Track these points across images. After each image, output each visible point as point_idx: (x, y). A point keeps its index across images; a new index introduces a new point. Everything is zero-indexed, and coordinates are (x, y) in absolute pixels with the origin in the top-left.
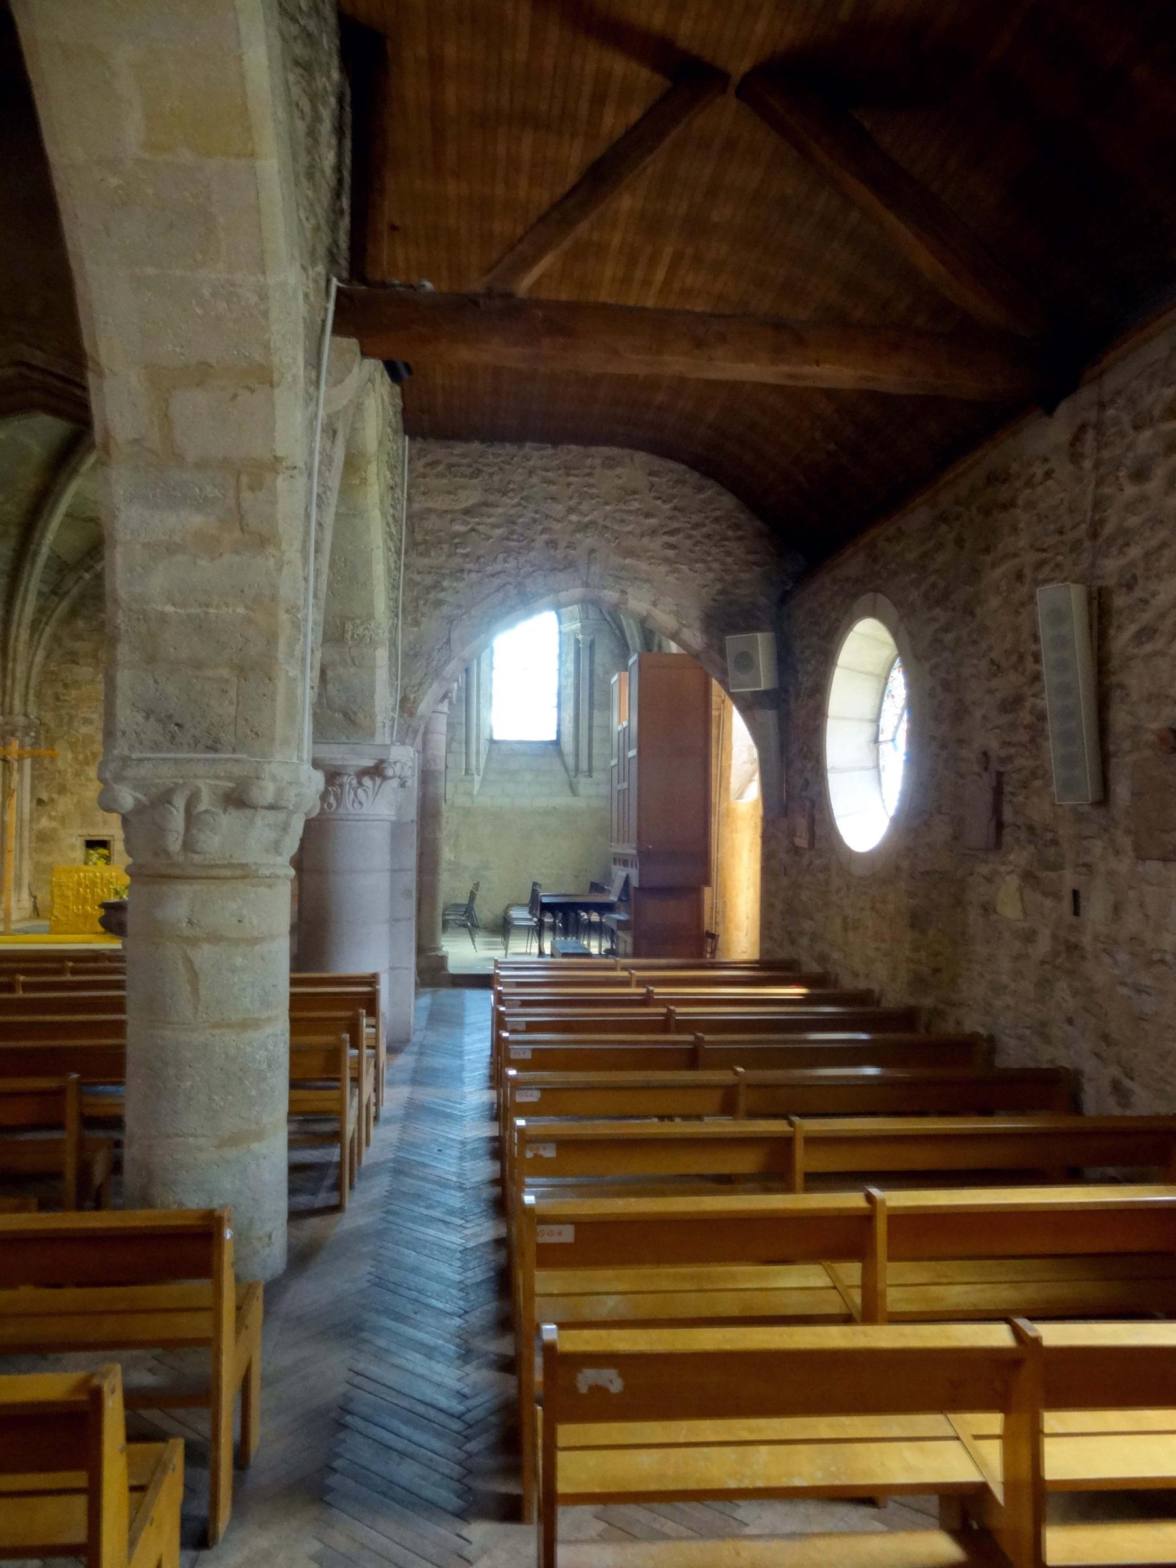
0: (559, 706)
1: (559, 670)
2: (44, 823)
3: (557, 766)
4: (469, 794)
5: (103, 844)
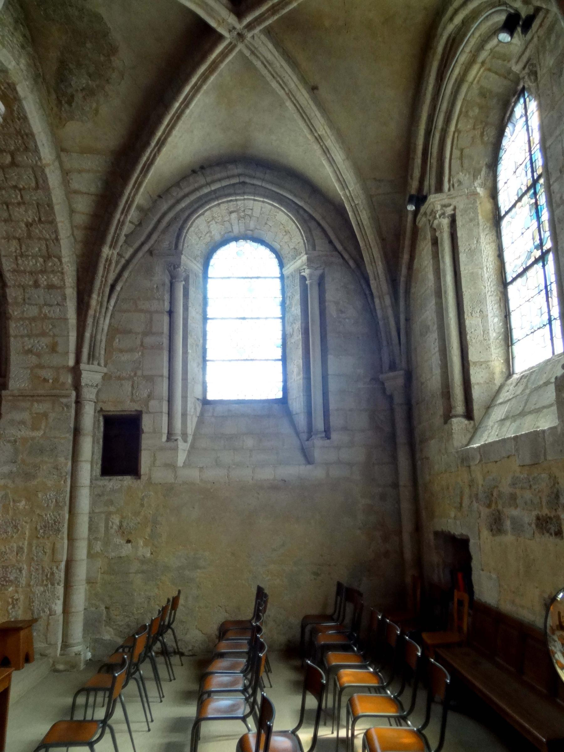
0: (284, 359)
1: (283, 318)
3: (285, 429)
4: (172, 466)
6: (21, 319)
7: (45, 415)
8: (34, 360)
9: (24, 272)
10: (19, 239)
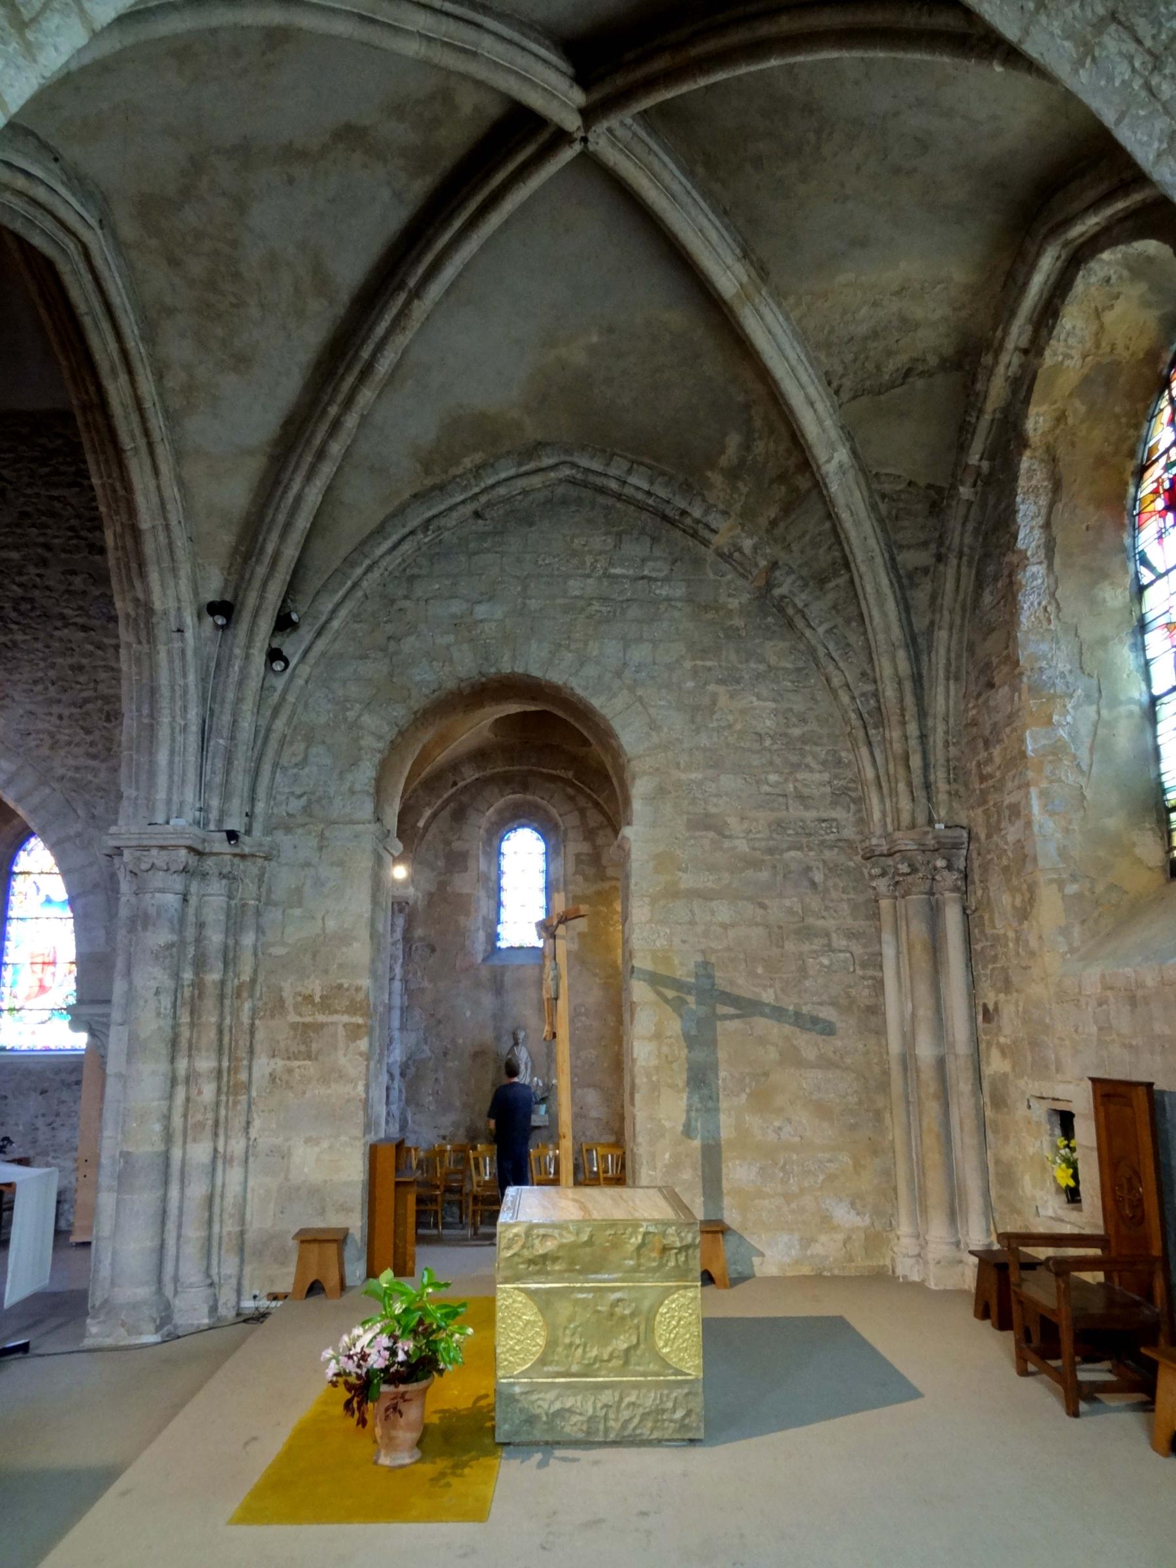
10: (1113, 17)
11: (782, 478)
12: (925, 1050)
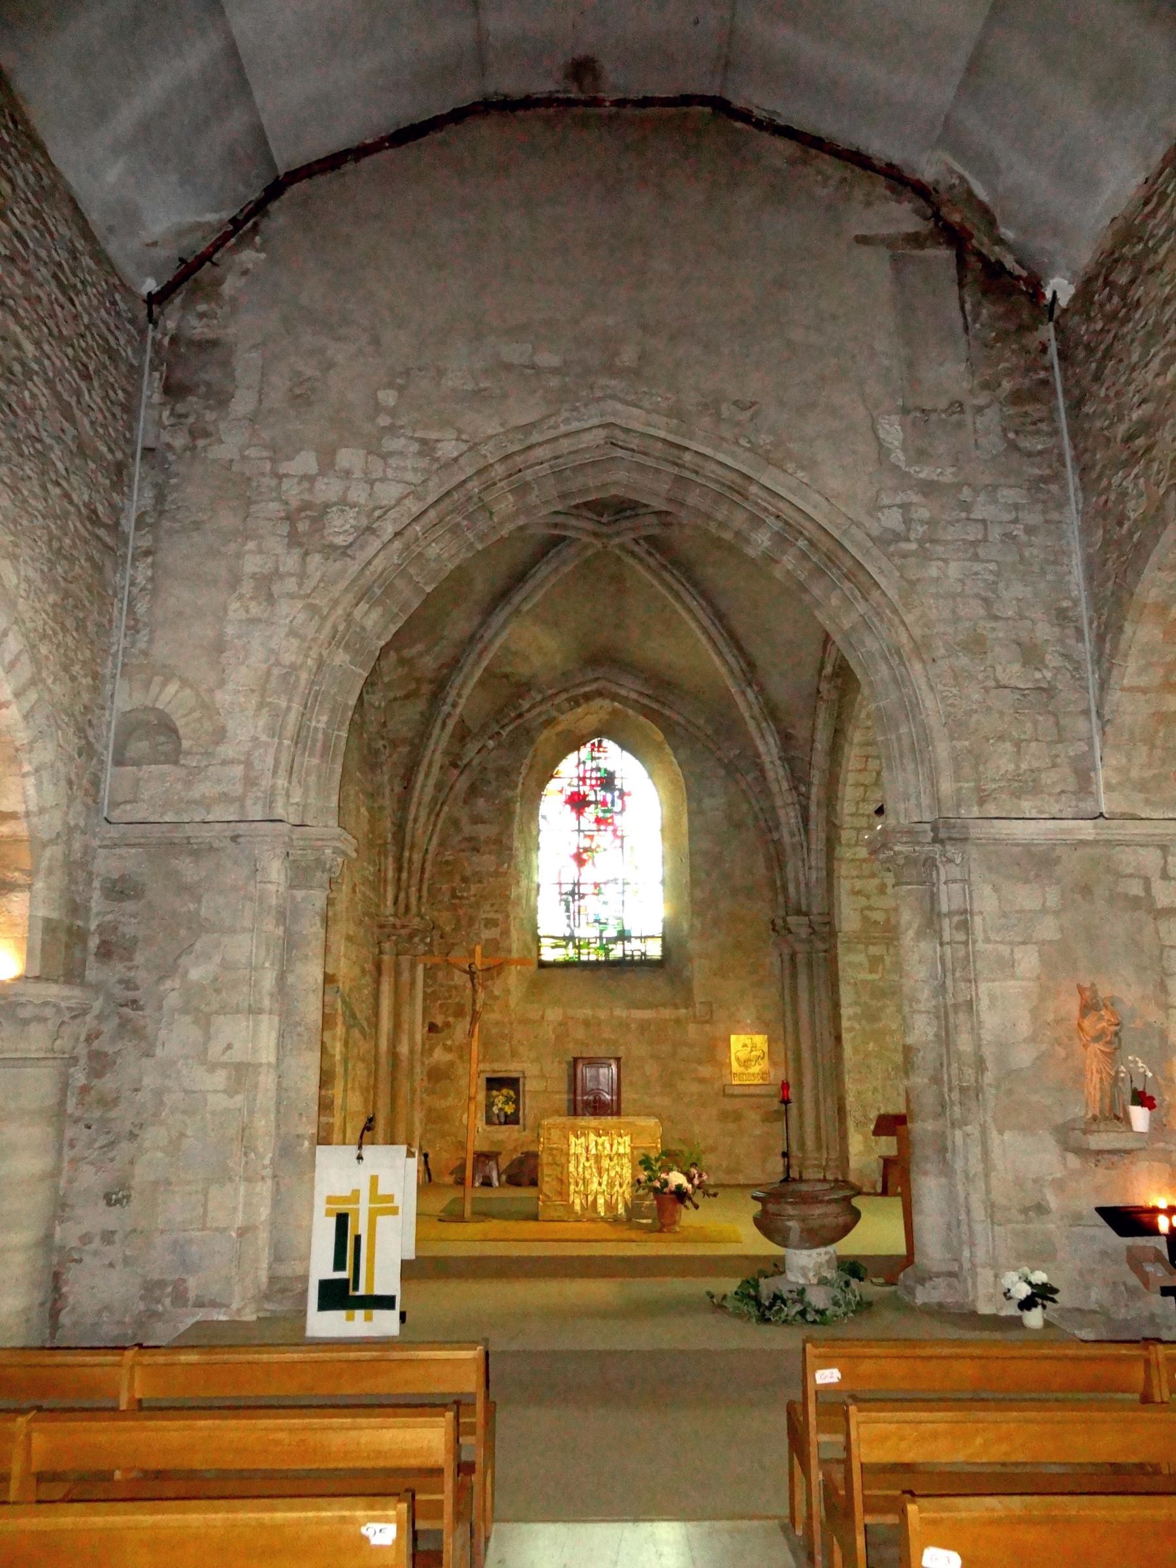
2: (439, 1056)
5: (512, 1083)
6: (852, 860)
7: (881, 959)
8: (863, 902)
9: (863, 815)
11: (418, 681)
12: (404, 1049)
